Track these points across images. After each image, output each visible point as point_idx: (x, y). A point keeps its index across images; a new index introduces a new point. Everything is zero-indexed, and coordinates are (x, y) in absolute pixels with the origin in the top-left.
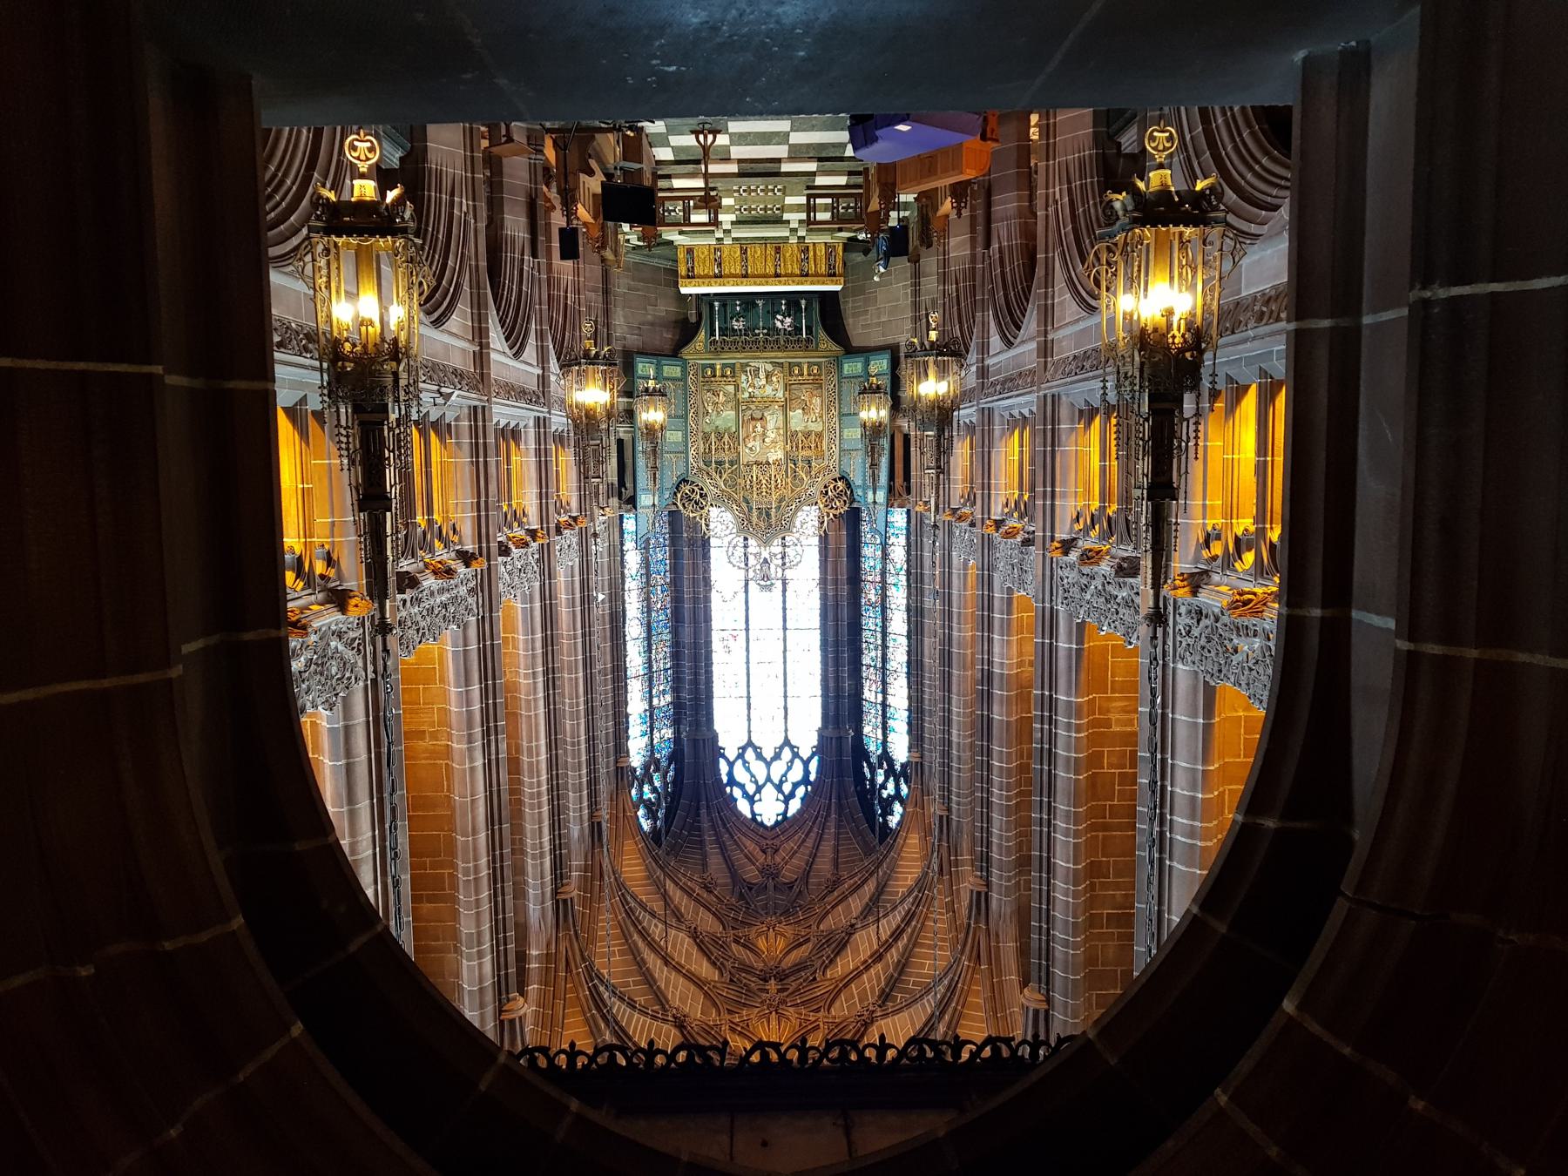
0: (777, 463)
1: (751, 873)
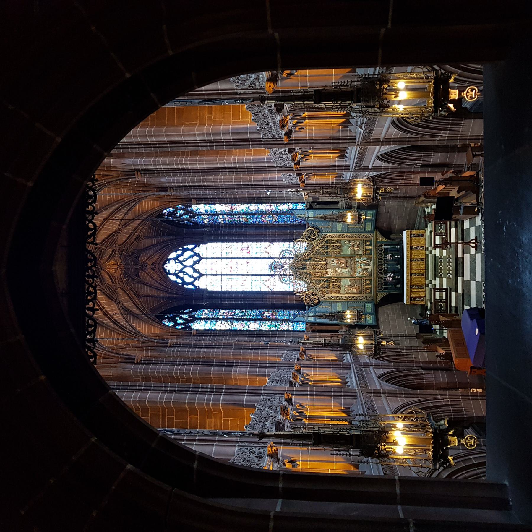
1: (143, 258)
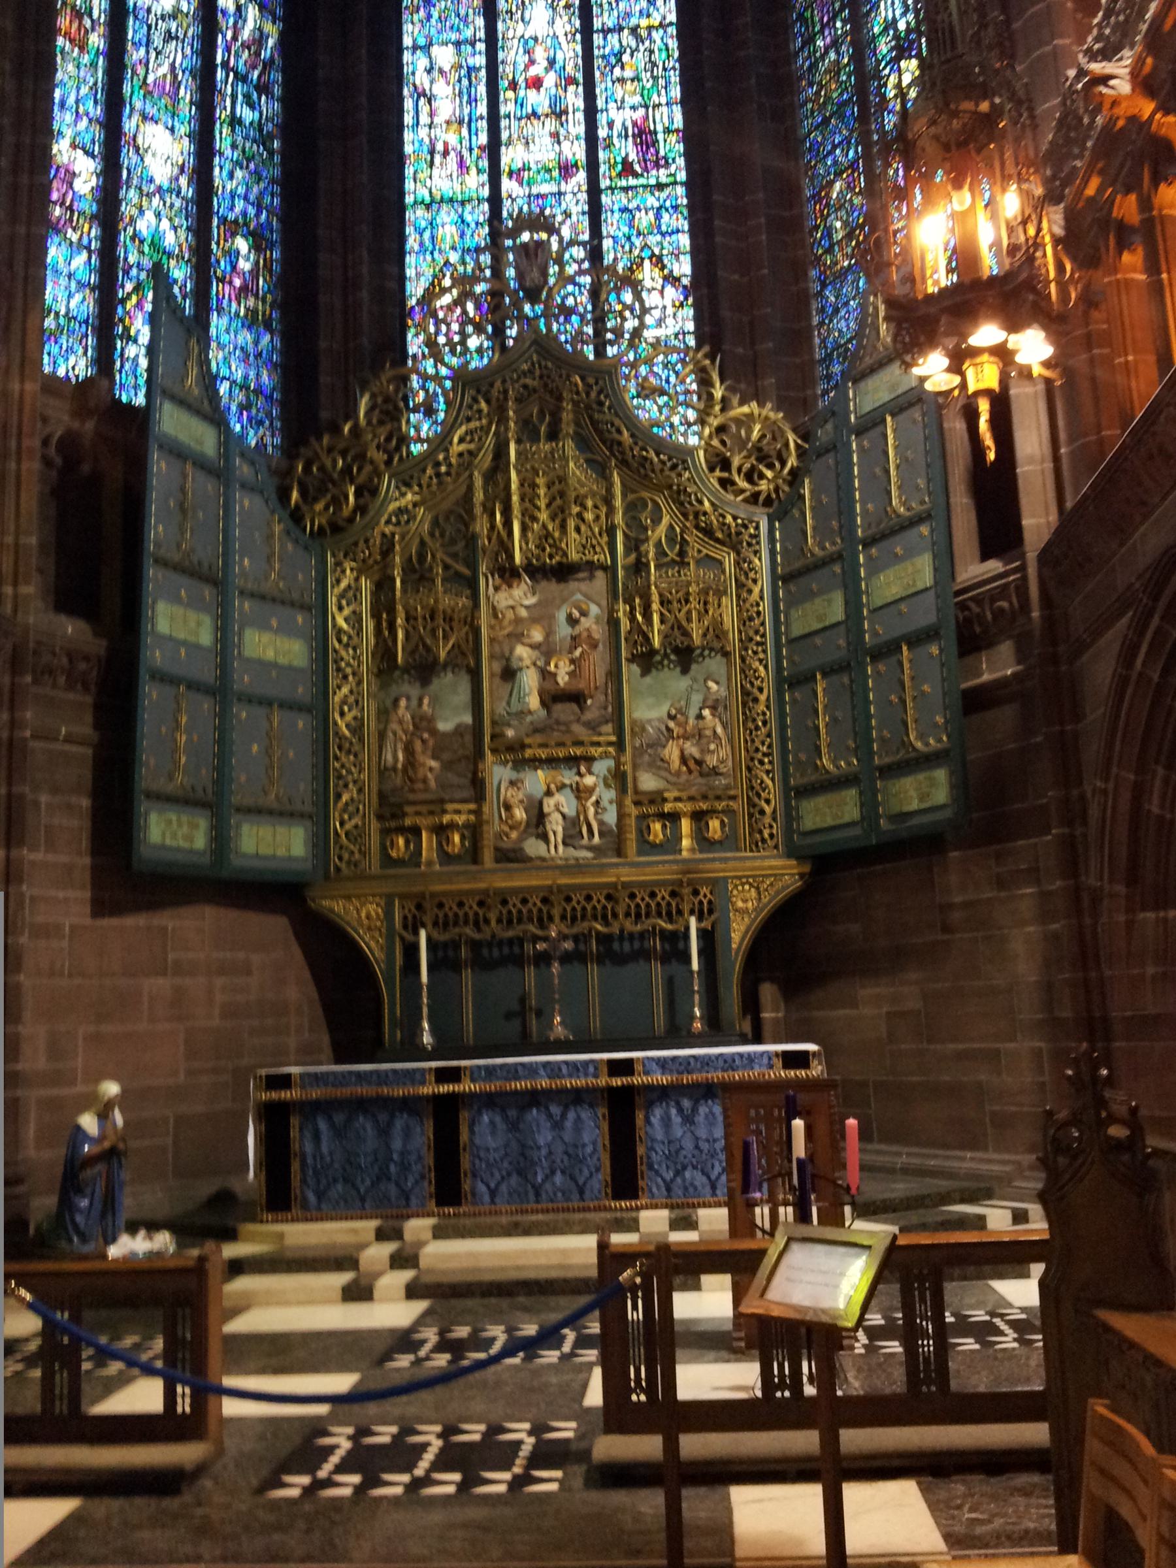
0: (508, 574)
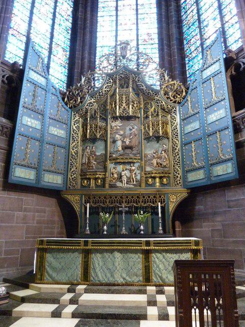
0: (115, 118)
